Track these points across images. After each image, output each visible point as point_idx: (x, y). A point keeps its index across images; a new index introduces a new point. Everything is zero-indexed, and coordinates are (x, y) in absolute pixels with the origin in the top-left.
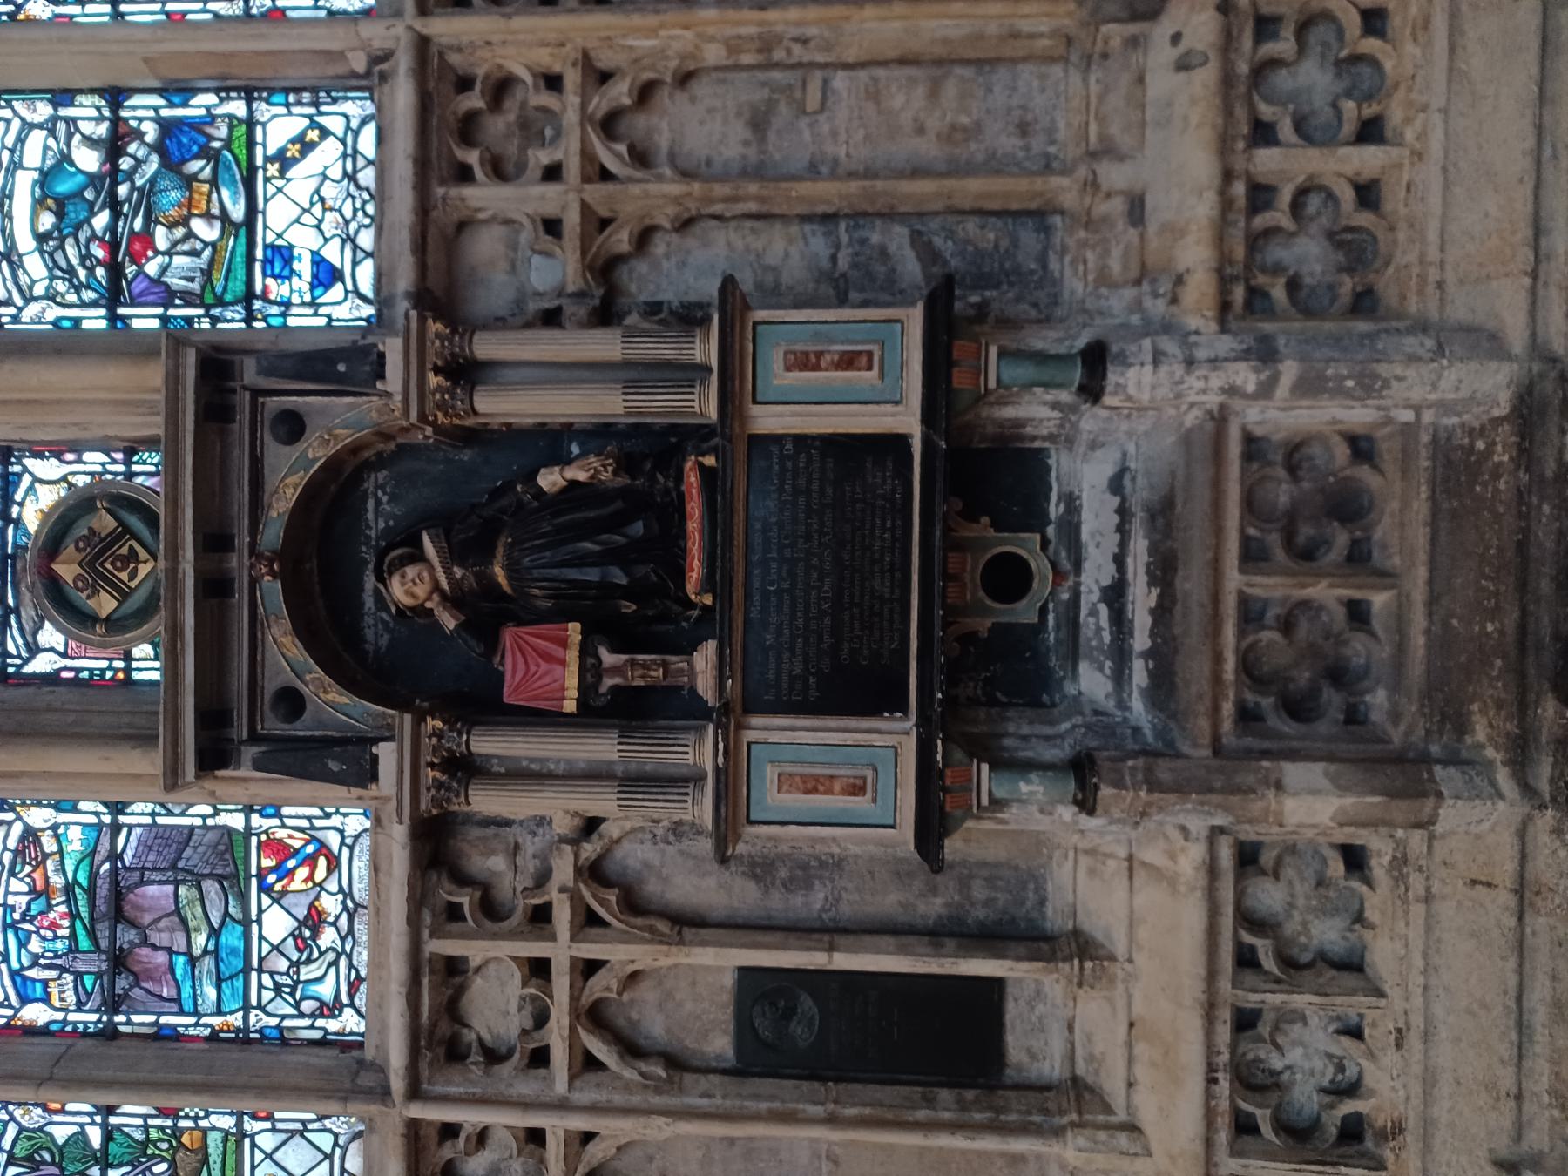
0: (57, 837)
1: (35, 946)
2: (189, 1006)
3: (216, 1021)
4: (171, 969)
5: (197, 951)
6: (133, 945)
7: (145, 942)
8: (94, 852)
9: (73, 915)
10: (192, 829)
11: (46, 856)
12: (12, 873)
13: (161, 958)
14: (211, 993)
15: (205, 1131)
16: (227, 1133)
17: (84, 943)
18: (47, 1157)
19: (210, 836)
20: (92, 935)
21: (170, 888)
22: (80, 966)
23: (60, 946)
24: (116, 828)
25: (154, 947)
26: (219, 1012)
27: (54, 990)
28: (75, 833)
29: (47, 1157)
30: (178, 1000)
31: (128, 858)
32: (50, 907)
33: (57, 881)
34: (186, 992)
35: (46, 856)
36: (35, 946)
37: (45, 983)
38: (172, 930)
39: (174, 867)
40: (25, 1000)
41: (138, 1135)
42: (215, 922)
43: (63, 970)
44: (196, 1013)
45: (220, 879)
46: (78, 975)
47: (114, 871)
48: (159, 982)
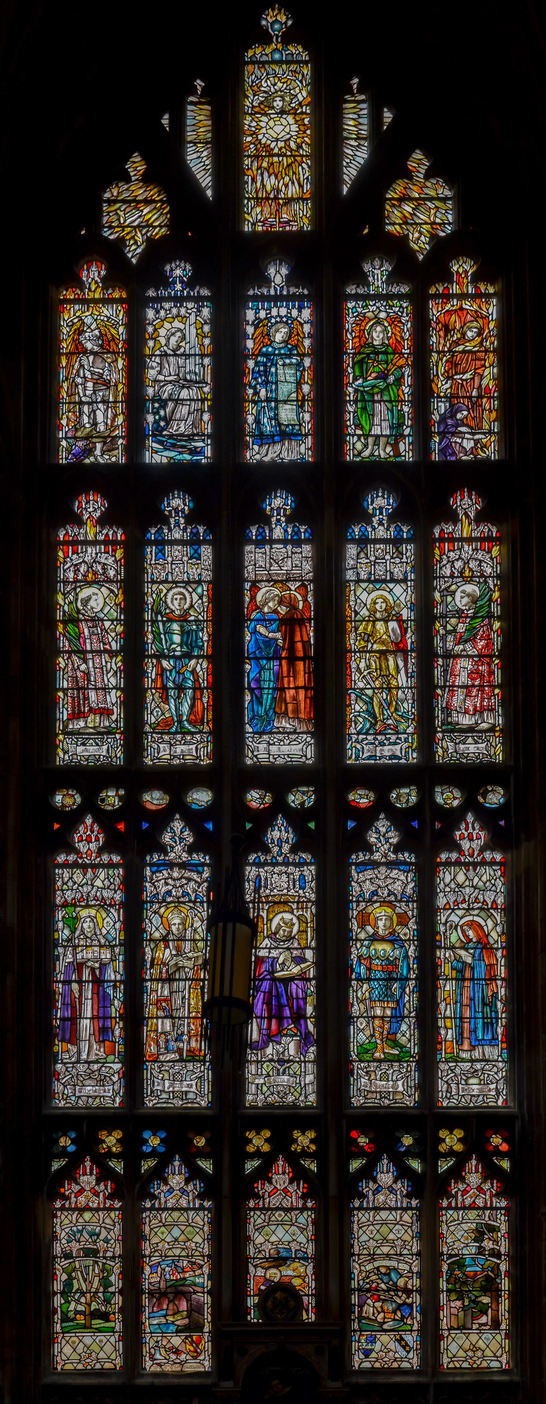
0: (200, 1275)
1: (167, 1269)
2: (151, 1315)
3: (147, 1324)
4: (162, 1310)
5: (167, 1318)
6: (168, 1298)
7: (169, 1302)
8: (195, 1285)
9: (177, 1280)
10: (204, 1315)
11: (194, 1271)
12: (189, 1262)
13: (165, 1307)
14: (155, 1322)
15: (115, 1321)
16: (114, 1328)
17: (169, 1284)
18: (105, 1274)
19: (202, 1321)
20: (170, 1286)
21: (185, 1309)
22: (162, 1283)
23: (168, 1277)
24: (203, 1293)
25: (168, 1305)
26: (149, 1325)
27: (155, 1275)
28: (201, 1280)
29: (105, 1274)
30: (153, 1312)
31: (194, 1296)
32: (179, 1273)
33: (187, 1275)
34: (156, 1315)
35: (194, 1271)
36: (167, 1269)
37: (157, 1273)
38: (173, 1309)
39: (192, 1310)
40: (151, 1266)
41: (113, 1302)
42: (176, 1323)
43: (161, 1278)
44: (149, 1318)
45: (189, 1323)
46: (159, 1282)
47: (191, 1293)
48: (158, 1306)
